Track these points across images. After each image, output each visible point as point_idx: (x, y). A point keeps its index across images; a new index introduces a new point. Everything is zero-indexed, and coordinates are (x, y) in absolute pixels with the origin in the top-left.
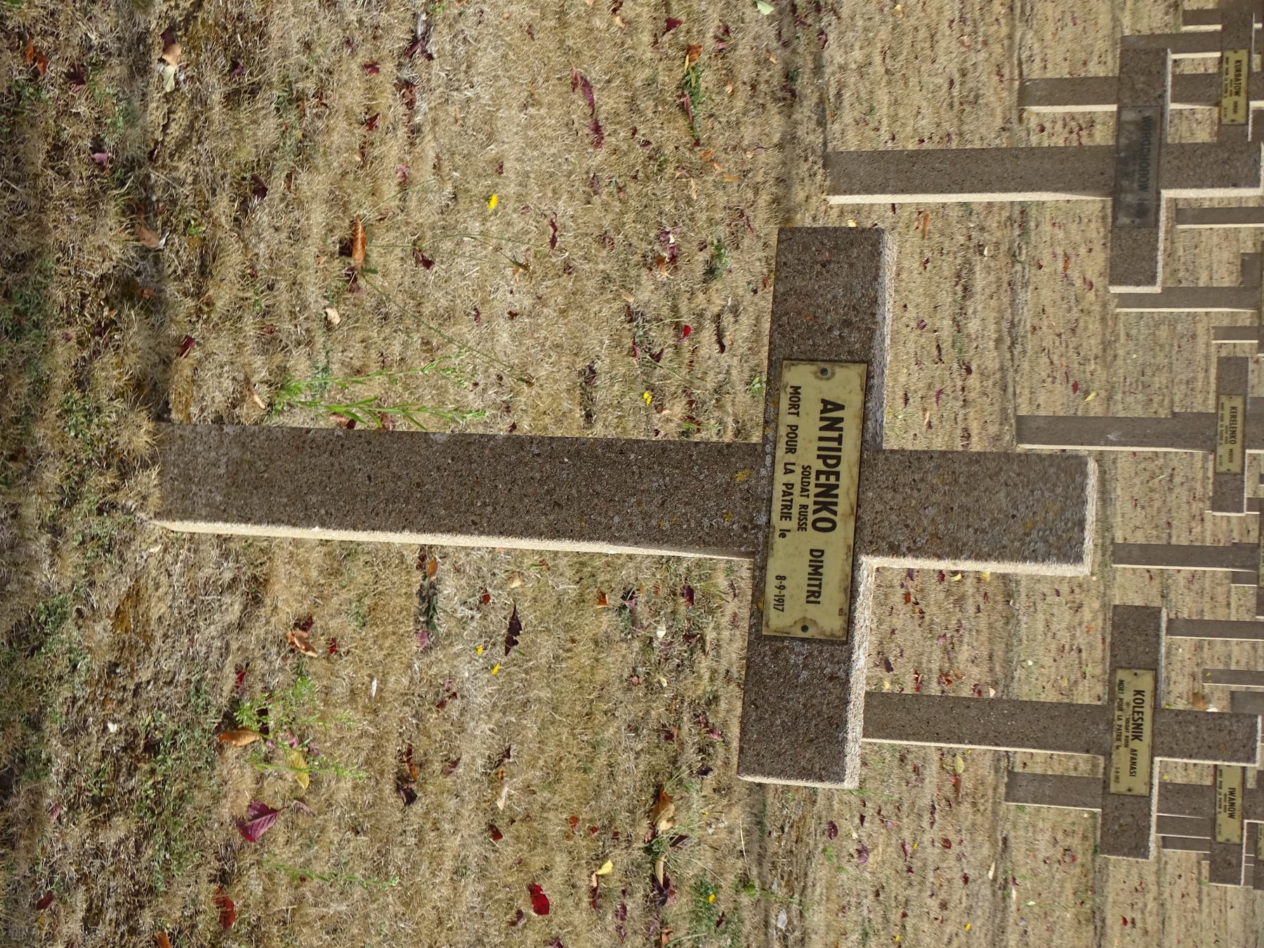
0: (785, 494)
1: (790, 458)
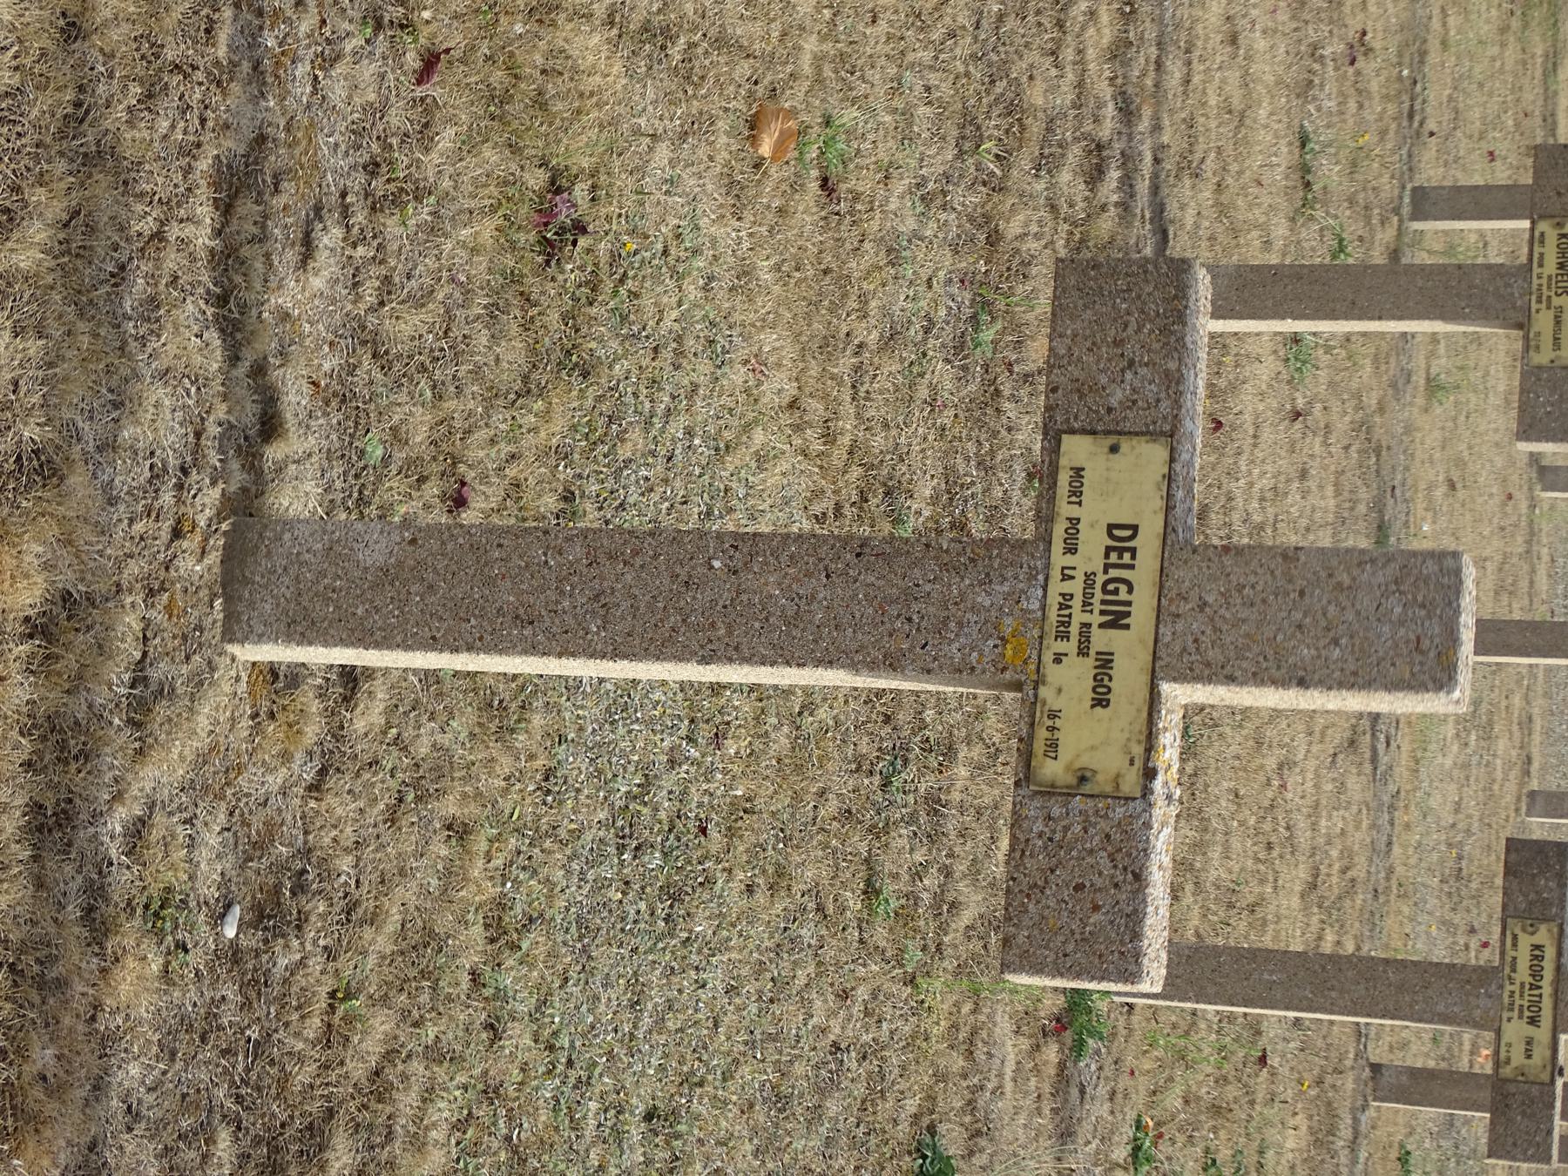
0: (1061, 607)
1: (1069, 560)
